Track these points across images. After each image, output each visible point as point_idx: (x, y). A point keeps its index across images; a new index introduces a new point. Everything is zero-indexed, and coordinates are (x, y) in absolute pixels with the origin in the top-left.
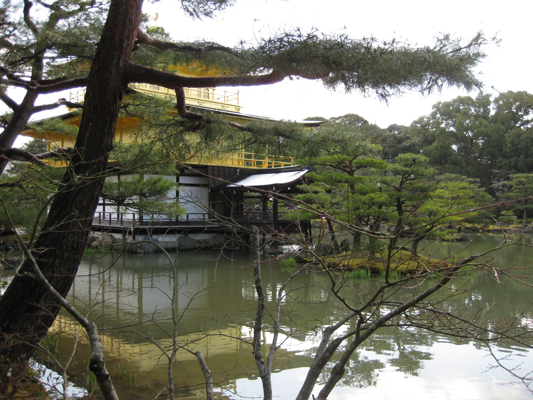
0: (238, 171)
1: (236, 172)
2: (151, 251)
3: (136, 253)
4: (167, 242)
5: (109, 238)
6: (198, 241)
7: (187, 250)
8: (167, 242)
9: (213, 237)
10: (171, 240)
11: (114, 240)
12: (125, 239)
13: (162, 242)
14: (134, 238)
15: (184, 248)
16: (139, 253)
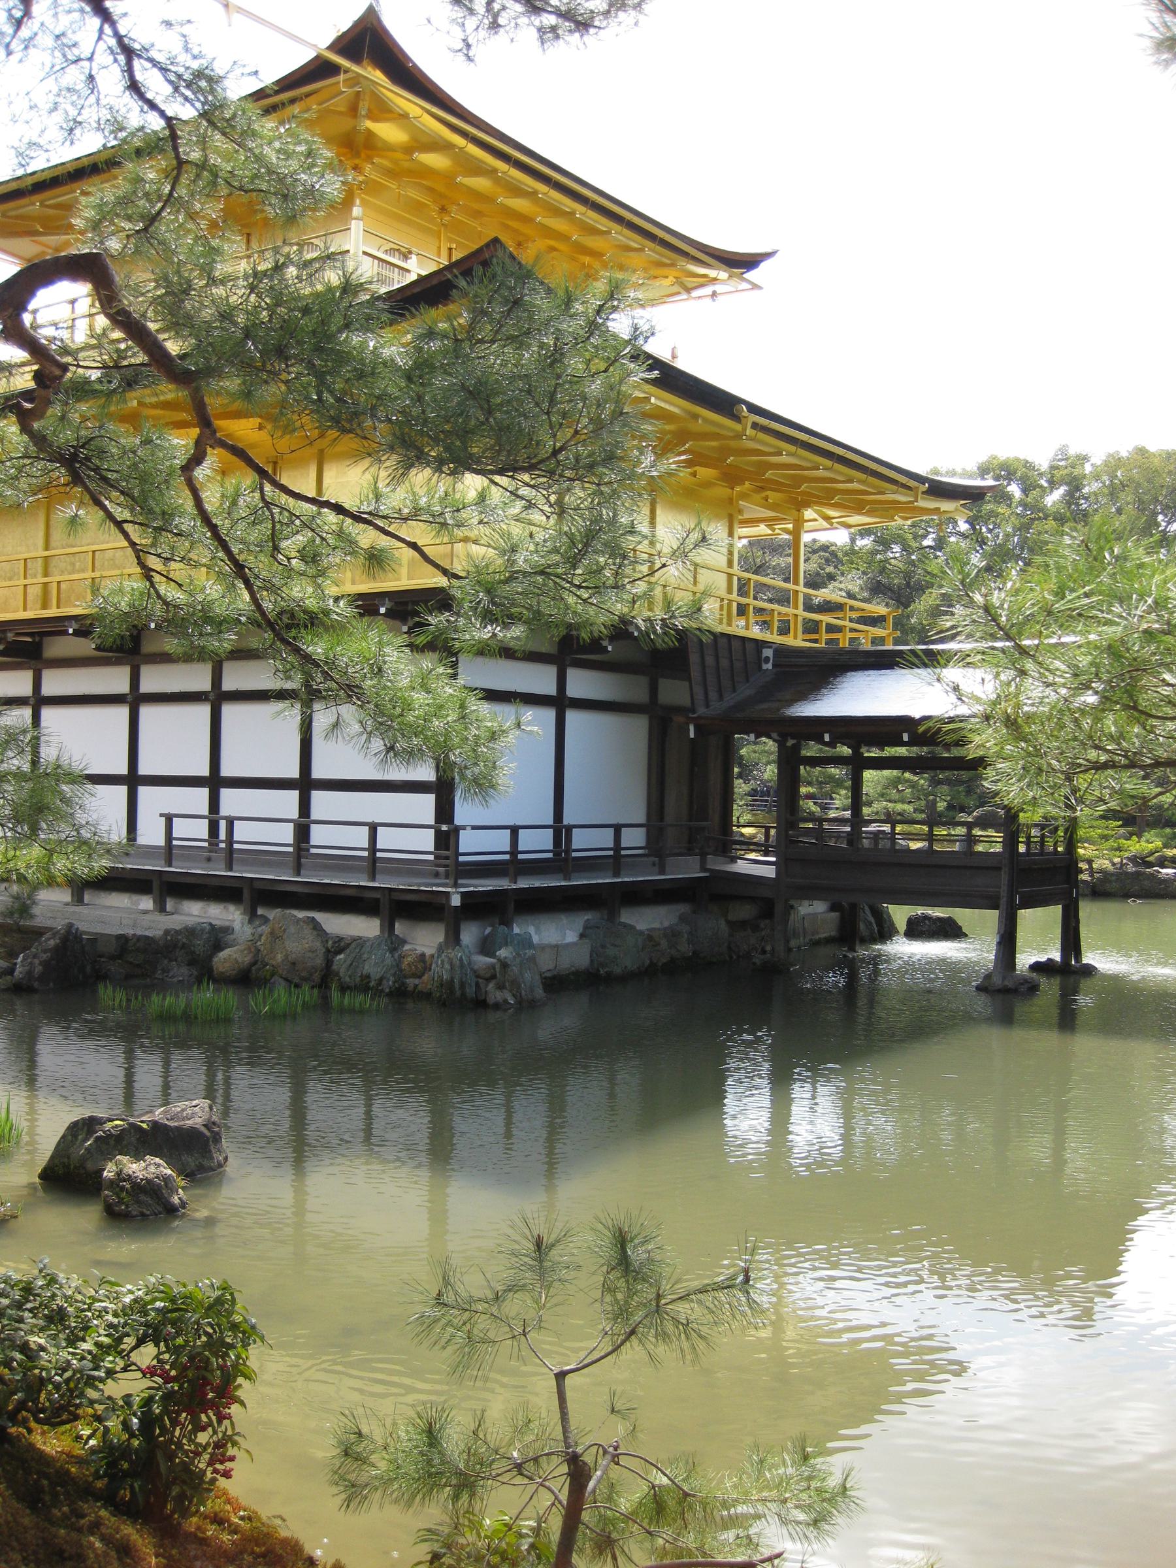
0: (768, 653)
1: (759, 660)
2: (540, 993)
3: (481, 1004)
4: (557, 946)
5: (307, 931)
6: (650, 938)
7: (625, 978)
8: (556, 948)
9: (682, 919)
10: (557, 937)
11: (340, 945)
12: (395, 944)
13: (543, 948)
14: (454, 937)
15: (618, 970)
16: (497, 1006)
